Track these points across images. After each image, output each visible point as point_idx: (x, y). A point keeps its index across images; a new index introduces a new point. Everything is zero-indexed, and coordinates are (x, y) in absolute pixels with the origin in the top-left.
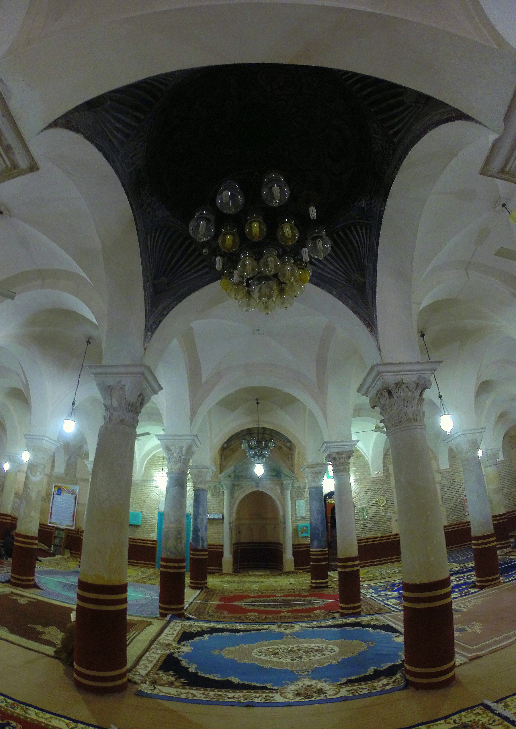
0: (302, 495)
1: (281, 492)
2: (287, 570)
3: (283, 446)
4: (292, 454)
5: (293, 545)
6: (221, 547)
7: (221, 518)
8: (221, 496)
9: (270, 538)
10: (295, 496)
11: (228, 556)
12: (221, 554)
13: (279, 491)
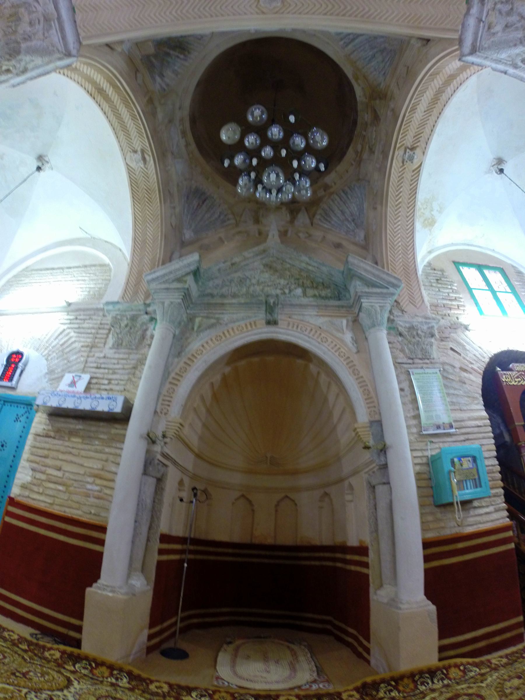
0: (426, 357)
1: (355, 341)
3: (344, 243)
5: (426, 545)
9: (312, 528)
10: (402, 358)
13: (348, 337)
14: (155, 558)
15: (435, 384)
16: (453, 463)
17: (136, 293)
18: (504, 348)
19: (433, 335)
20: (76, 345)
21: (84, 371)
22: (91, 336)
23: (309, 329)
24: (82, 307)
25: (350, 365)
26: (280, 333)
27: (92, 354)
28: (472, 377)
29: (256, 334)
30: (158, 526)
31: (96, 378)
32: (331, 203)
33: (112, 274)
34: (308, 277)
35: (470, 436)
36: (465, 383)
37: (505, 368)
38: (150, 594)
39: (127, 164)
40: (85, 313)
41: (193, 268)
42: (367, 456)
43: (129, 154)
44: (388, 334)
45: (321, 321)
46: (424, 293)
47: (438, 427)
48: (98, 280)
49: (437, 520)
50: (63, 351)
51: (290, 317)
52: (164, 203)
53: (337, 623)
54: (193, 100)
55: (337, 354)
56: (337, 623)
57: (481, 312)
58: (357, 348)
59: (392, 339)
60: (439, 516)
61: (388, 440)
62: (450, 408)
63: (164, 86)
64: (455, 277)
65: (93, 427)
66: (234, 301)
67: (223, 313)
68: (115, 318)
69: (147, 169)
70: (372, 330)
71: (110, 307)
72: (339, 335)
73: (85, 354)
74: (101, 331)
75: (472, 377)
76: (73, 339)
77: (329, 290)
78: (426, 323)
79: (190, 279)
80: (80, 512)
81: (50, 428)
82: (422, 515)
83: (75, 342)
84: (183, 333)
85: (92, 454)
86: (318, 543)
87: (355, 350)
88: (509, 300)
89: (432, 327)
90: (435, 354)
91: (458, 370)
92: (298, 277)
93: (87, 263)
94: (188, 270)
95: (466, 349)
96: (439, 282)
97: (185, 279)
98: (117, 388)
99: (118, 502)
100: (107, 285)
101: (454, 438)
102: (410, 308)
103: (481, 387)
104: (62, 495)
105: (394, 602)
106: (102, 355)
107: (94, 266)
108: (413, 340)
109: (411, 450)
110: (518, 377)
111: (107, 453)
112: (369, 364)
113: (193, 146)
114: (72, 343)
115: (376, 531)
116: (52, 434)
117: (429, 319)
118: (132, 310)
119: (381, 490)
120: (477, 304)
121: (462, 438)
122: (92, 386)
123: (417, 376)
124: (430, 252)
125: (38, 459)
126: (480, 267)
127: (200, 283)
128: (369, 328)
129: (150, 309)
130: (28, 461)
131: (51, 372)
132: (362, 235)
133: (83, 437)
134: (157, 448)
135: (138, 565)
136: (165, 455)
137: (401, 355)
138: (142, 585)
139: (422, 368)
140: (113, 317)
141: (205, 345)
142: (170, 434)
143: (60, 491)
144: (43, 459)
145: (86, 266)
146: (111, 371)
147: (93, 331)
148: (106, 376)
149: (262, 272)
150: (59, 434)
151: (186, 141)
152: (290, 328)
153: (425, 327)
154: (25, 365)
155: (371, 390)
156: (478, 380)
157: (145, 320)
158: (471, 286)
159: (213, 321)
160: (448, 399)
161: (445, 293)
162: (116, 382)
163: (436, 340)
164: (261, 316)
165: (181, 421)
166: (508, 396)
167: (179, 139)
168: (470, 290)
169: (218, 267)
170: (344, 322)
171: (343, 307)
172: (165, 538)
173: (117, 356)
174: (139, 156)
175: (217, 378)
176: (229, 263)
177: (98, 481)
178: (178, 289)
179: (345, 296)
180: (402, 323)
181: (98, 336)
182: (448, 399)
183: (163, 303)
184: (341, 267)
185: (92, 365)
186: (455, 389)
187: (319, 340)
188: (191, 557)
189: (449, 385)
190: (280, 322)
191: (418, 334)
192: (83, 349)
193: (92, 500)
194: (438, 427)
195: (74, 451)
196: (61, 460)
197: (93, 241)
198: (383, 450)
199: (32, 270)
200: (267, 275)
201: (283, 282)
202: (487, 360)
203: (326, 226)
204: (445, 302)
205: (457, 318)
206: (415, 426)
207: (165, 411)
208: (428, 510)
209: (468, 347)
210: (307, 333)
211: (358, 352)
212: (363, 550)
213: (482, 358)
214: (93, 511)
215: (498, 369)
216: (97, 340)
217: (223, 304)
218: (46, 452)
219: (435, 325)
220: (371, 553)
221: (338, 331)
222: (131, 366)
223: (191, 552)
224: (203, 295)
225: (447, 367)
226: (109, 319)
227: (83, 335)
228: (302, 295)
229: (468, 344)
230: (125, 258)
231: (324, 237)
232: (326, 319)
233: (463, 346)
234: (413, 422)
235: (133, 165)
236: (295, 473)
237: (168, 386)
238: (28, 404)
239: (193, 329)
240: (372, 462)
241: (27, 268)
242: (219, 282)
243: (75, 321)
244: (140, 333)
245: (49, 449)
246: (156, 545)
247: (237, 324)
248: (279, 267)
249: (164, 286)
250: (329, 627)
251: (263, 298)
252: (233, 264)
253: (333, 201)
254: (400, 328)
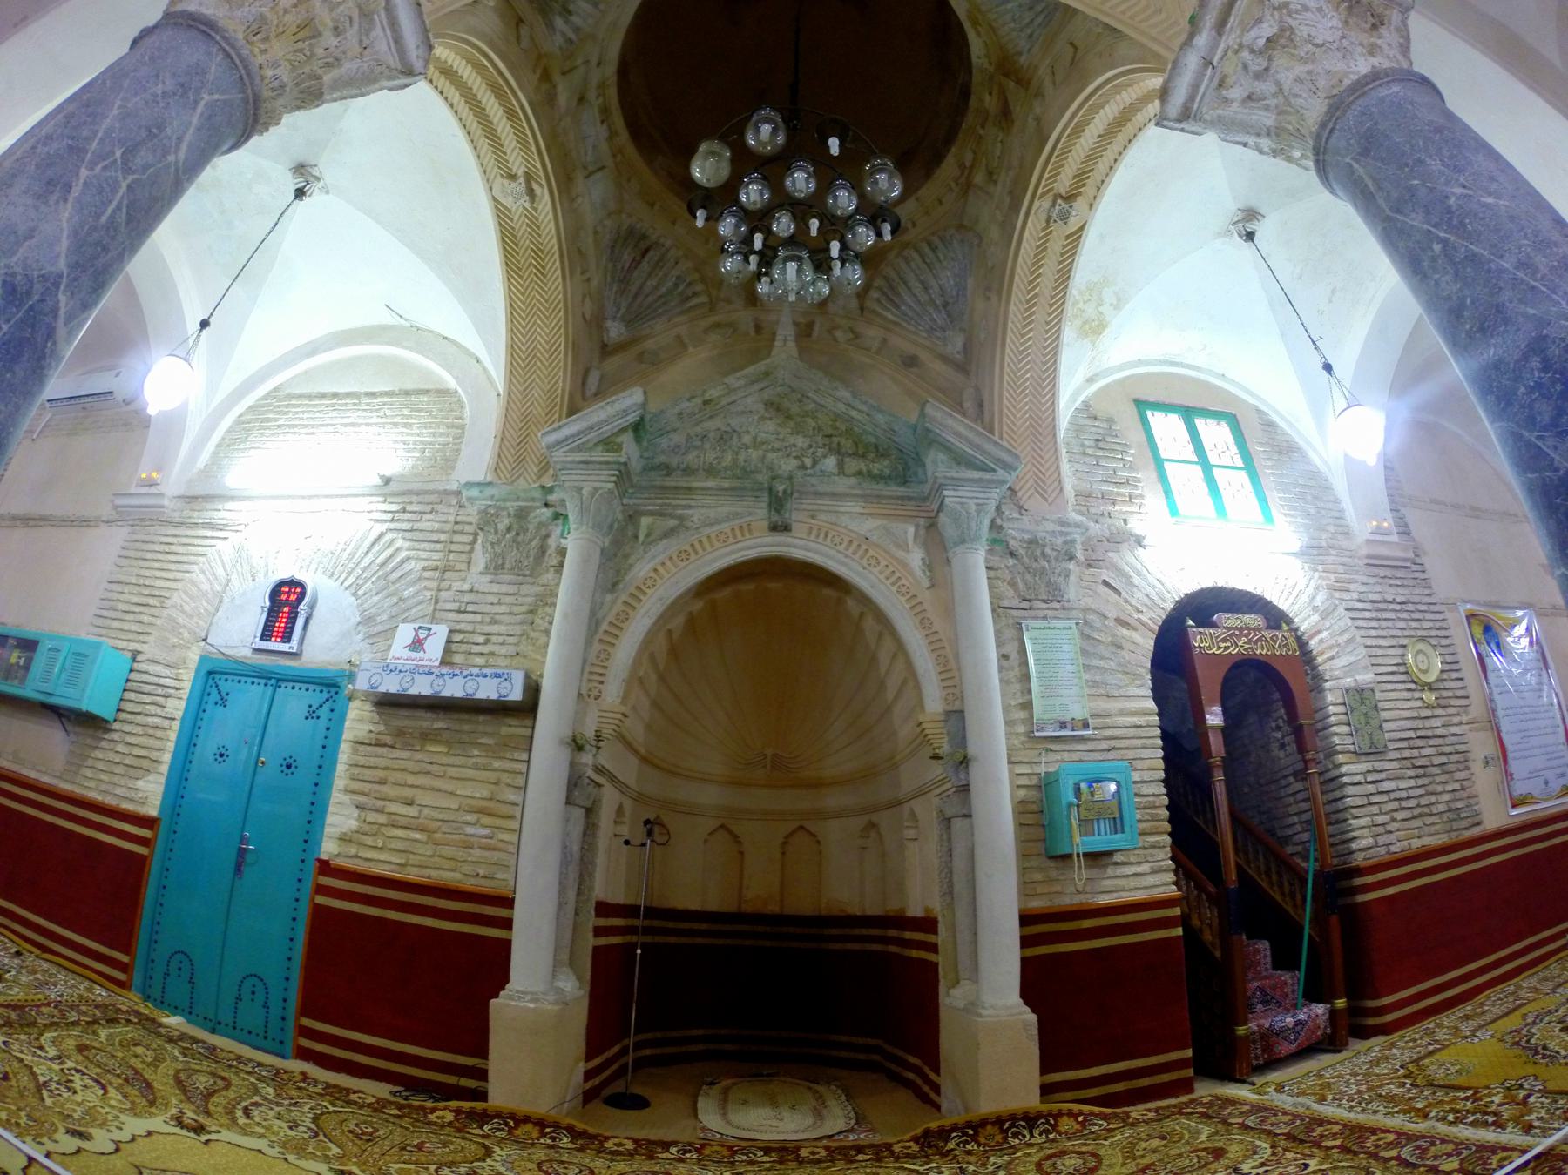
0: (1055, 596)
1: (929, 566)
2: (987, 1106)
3: (924, 356)
4: (977, 389)
5: (1026, 919)
6: (502, 912)
7: (516, 694)
8: (549, 577)
10: (1010, 599)
11: (540, 989)
12: (493, 965)
13: (916, 558)
14: (591, 941)
15: (1066, 648)
16: (1078, 790)
17: (520, 460)
18: (1208, 583)
19: (1072, 558)
20: (410, 565)
21: (434, 620)
22: (438, 546)
23: (847, 539)
24: (415, 487)
25: (917, 610)
26: (795, 546)
27: (446, 584)
28: (1136, 636)
29: (750, 548)
30: (591, 888)
31: (460, 631)
32: (903, 265)
33: (467, 412)
34: (849, 432)
35: (1117, 743)
36: (1121, 647)
37: (1205, 621)
38: (585, 1003)
39: (494, 199)
40: (420, 499)
41: (633, 418)
42: (937, 770)
43: (499, 179)
44: (990, 552)
45: (868, 526)
46: (1065, 467)
47: (1063, 726)
48: (438, 425)
49: (1049, 881)
50: (387, 578)
51: (813, 517)
52: (572, 275)
53: (889, 1048)
54: (624, 45)
55: (894, 589)
56: (889, 1048)
57: (1174, 511)
58: (931, 579)
59: (996, 561)
60: (1053, 873)
61: (972, 749)
62: (1087, 691)
63: (572, 36)
64: (1135, 436)
65: (465, 725)
66: (710, 483)
67: (690, 507)
68: (485, 512)
69: (536, 210)
70: (959, 549)
71: (475, 492)
72: (901, 554)
73: (434, 584)
74: (458, 538)
75: (1136, 636)
76: (404, 554)
77: (886, 463)
78: (1061, 533)
79: (627, 439)
80: (457, 876)
81: (382, 728)
82: (1023, 871)
83: (408, 558)
84: (617, 543)
85: (471, 773)
86: (856, 910)
87: (926, 584)
88: (1234, 482)
89: (1073, 541)
90: (1072, 592)
92: (830, 431)
93: (409, 386)
94: (623, 422)
95: (1131, 584)
96: (1101, 444)
97: (619, 440)
98: (503, 650)
99: (529, 853)
100: (460, 437)
101: (1090, 746)
102: (1033, 503)
103: (1150, 655)
104: (421, 849)
105: (972, 1007)
106: (466, 587)
107: (426, 392)
108: (1035, 565)
109: (1010, 762)
110: (1224, 640)
111: (495, 770)
112: (949, 610)
113: (624, 136)
114: (403, 562)
115: (949, 892)
116: (388, 740)
117: (1069, 525)
118: (518, 499)
119: (958, 824)
120: (1168, 493)
121: (1104, 745)
122: (454, 647)
123: (1035, 633)
124: (1091, 380)
125: (367, 787)
126: (1189, 413)
127: (645, 444)
128: (956, 544)
129: (552, 498)
130: (347, 791)
131: (368, 620)
132: (959, 341)
133: (448, 743)
134: (587, 759)
135: (565, 957)
136: (599, 770)
137: (1010, 593)
138: (573, 987)
139: (1045, 618)
140: (480, 512)
141: (660, 569)
142: (606, 733)
143: (416, 840)
144: (376, 787)
145: (407, 393)
146: (487, 619)
147: (443, 537)
148: (479, 628)
149: (763, 418)
150: (401, 739)
151: (609, 127)
152: (812, 537)
153: (1059, 541)
154: (312, 607)
155: (951, 657)
156: (1148, 644)
157: (544, 519)
158: (1163, 456)
159: (672, 523)
160: (1086, 676)
161: (1107, 468)
162: (500, 639)
163: (1078, 564)
164: (760, 512)
165: (623, 709)
166: (1199, 673)
167: (597, 134)
168: (1159, 463)
169: (677, 410)
170: (911, 530)
171: (910, 499)
172: (603, 909)
173: (495, 588)
174: (519, 186)
175: (678, 622)
176: (698, 401)
177: (486, 820)
178: (607, 463)
179: (916, 474)
180: (1017, 530)
181: (454, 547)
182: (1086, 676)
183: (579, 490)
184: (913, 418)
185: (449, 606)
186: (1102, 658)
187: (864, 562)
188: (648, 939)
189: (1091, 650)
190: (794, 525)
191: (1043, 554)
192: (426, 574)
193: (478, 852)
194: (1063, 726)
195: (434, 768)
196: (412, 786)
197: (414, 336)
198: (964, 762)
199: (291, 396)
200: (770, 426)
201: (801, 442)
202: (1170, 606)
203: (889, 316)
204: (1105, 488)
205: (1125, 521)
206: (1023, 722)
207: (595, 692)
208: (1034, 862)
209: (1136, 580)
210: (841, 548)
211: (932, 586)
212: (928, 924)
213: (1159, 602)
214: (482, 873)
215: (1191, 623)
216: (452, 556)
217: (690, 489)
218: (381, 774)
219: (1077, 537)
220: (941, 928)
221: (899, 546)
222: (524, 609)
223: (647, 931)
224: (649, 468)
225: (1090, 617)
226: (472, 514)
227: (423, 545)
228: (835, 471)
229: (1139, 574)
230: (490, 380)
231: (885, 340)
232: (877, 522)
233: (1128, 578)
234: (1022, 715)
235: (508, 201)
236: (817, 785)
237: (597, 646)
238: (330, 686)
239: (636, 537)
240: (945, 780)
241: (276, 389)
242: (677, 438)
243: (402, 516)
244: (535, 543)
245: (386, 768)
246: (591, 921)
247: (717, 528)
248: (795, 409)
249: (579, 457)
250: (876, 1057)
251: (763, 478)
252: (706, 403)
253: (908, 263)
254: (1012, 543)
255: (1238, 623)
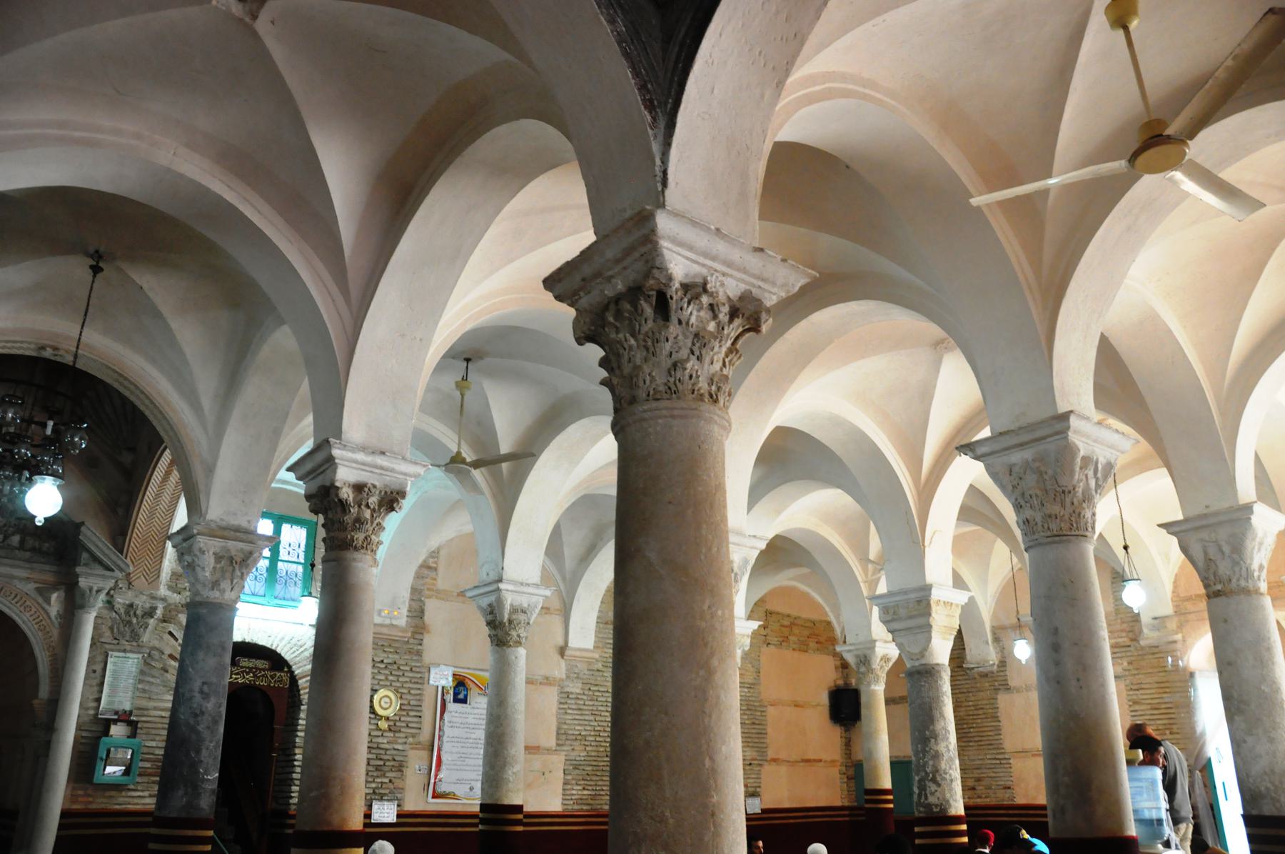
0: (135, 636)
10: (107, 636)
49: (87, 795)
91: (165, 657)
137: (108, 634)
139: (124, 651)
234: (94, 704)
255: (251, 665)
